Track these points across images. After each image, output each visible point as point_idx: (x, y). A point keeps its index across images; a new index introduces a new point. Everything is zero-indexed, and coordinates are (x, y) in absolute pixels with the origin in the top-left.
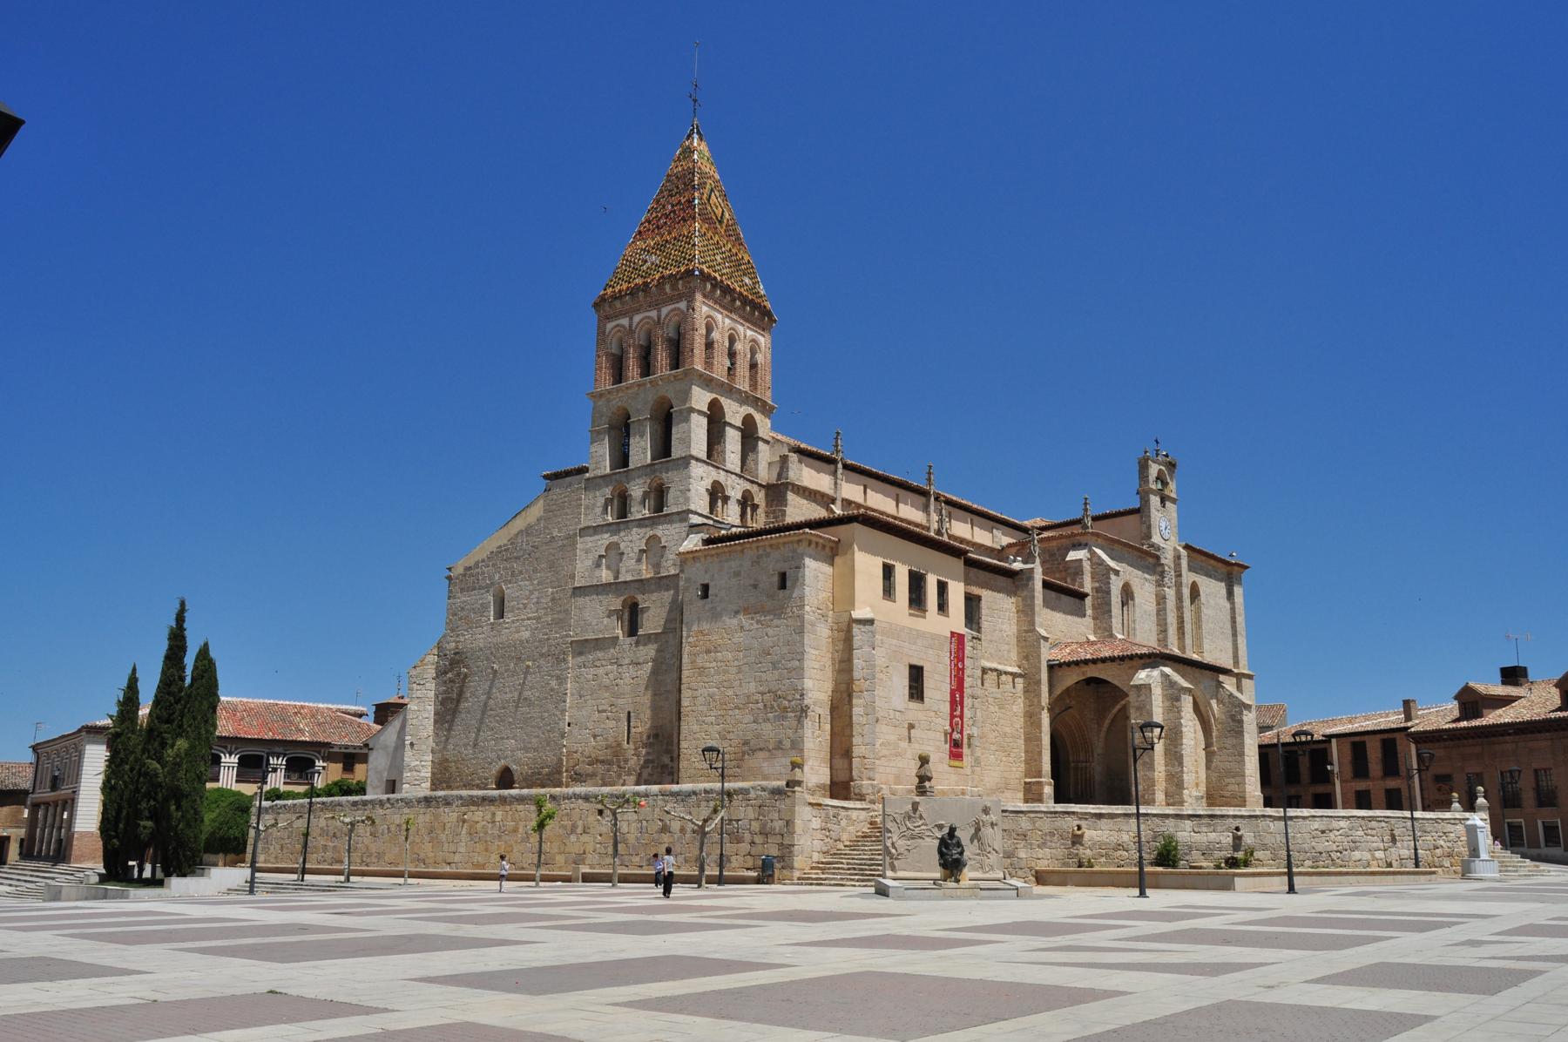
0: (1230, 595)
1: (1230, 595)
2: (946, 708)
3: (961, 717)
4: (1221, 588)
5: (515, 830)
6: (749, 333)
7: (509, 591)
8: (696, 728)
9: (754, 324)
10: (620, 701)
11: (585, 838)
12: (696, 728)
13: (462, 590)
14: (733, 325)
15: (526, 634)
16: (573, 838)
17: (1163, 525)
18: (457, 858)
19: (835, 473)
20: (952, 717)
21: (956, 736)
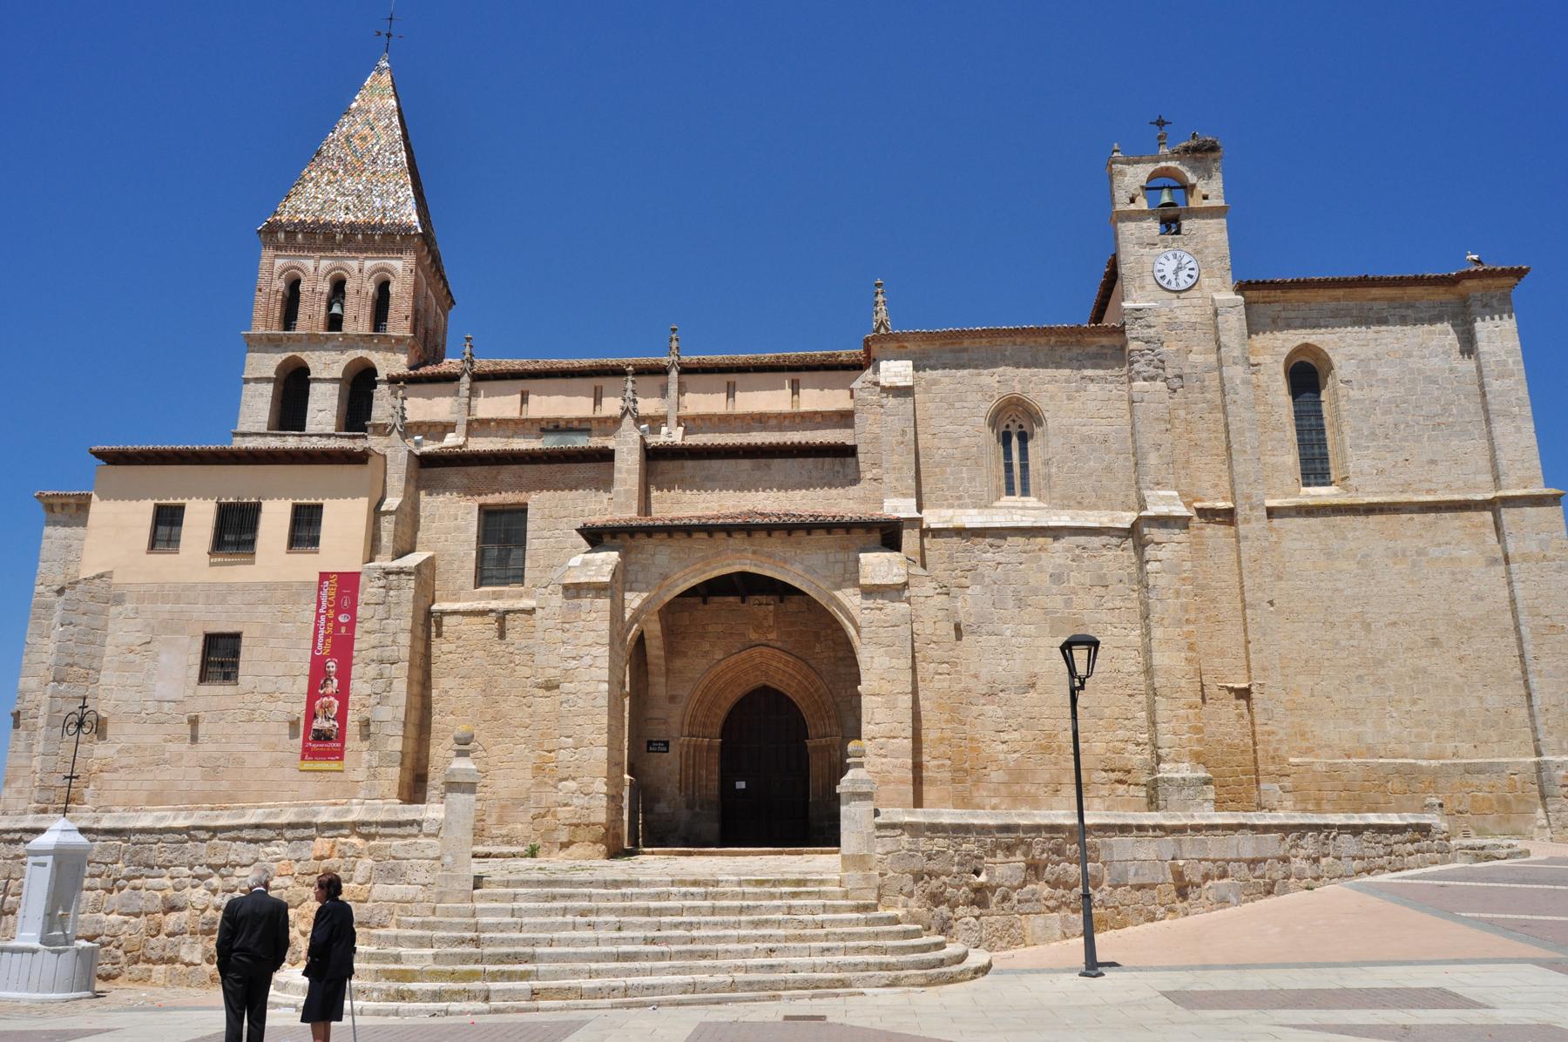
0: (1468, 345)
1: (1468, 345)
2: (303, 684)
3: (343, 694)
4: (1444, 335)
6: (369, 264)
9: (383, 250)
14: (336, 263)
17: (1169, 267)
19: (457, 393)
20: (313, 695)
21: (319, 724)
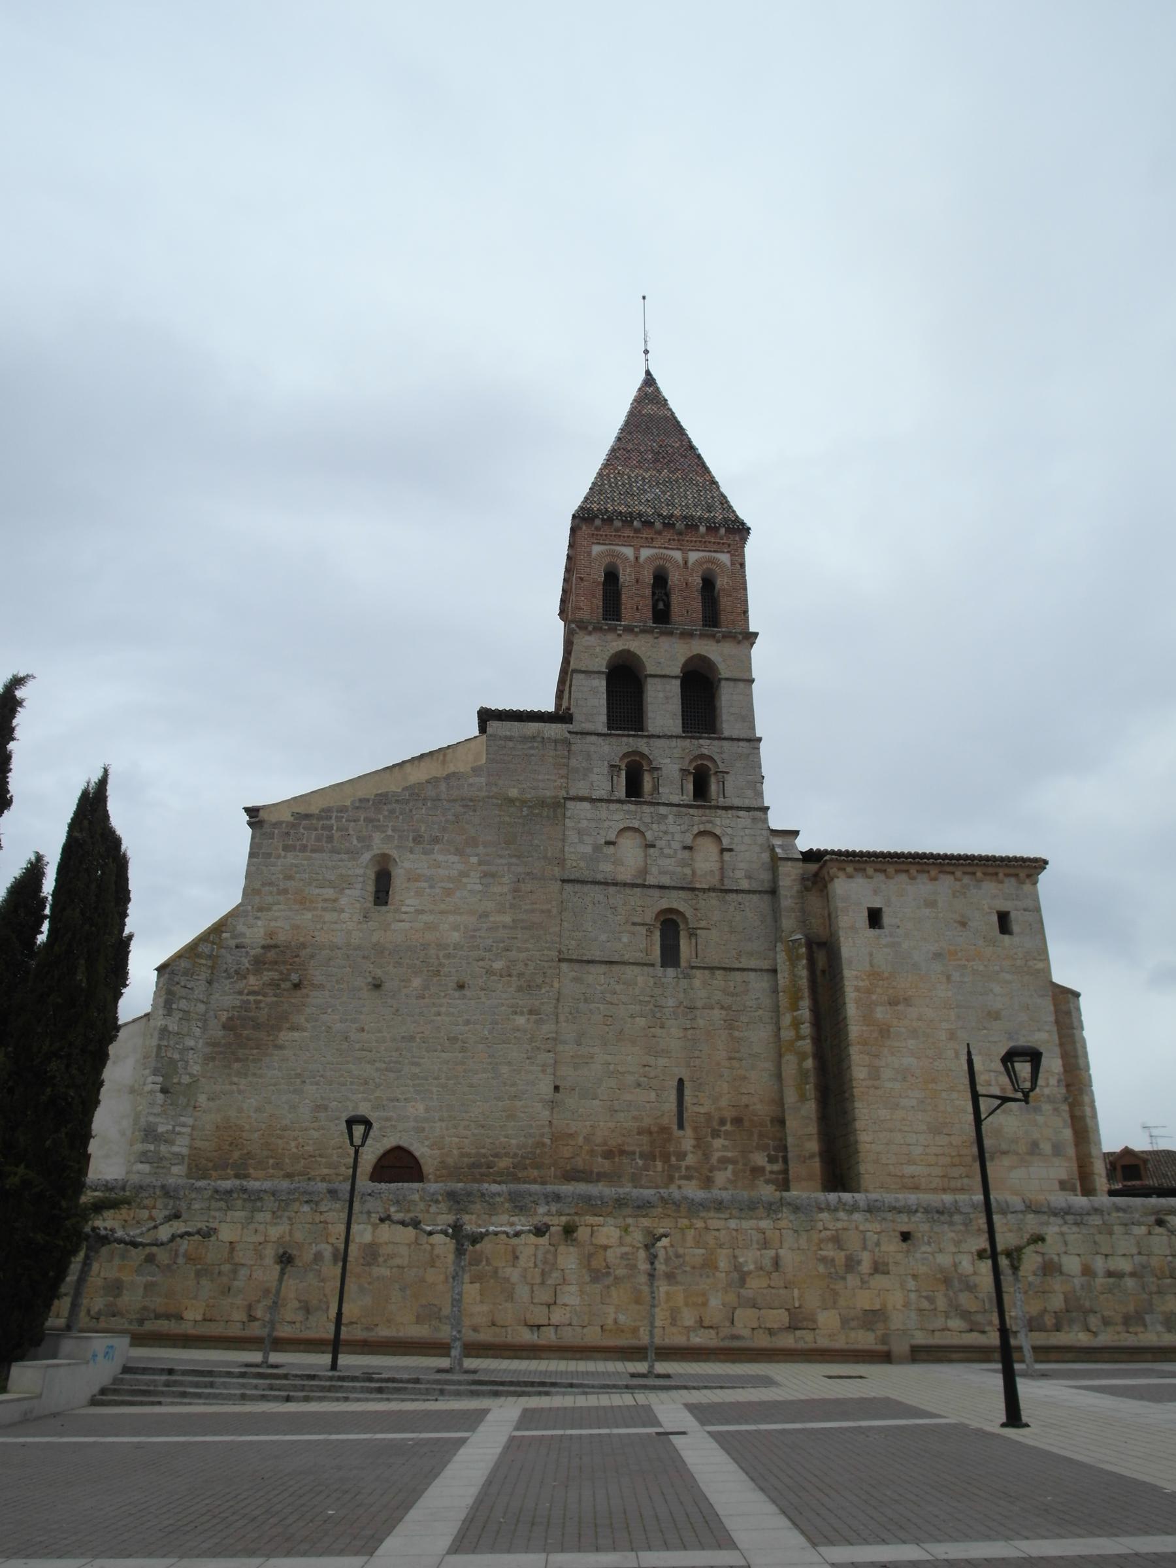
5: (709, 1265)
7: (405, 866)
8: (884, 1113)
10: (662, 1062)
11: (879, 1281)
12: (884, 1113)
13: (286, 848)
15: (455, 936)
16: (852, 1280)
18: (557, 1316)
